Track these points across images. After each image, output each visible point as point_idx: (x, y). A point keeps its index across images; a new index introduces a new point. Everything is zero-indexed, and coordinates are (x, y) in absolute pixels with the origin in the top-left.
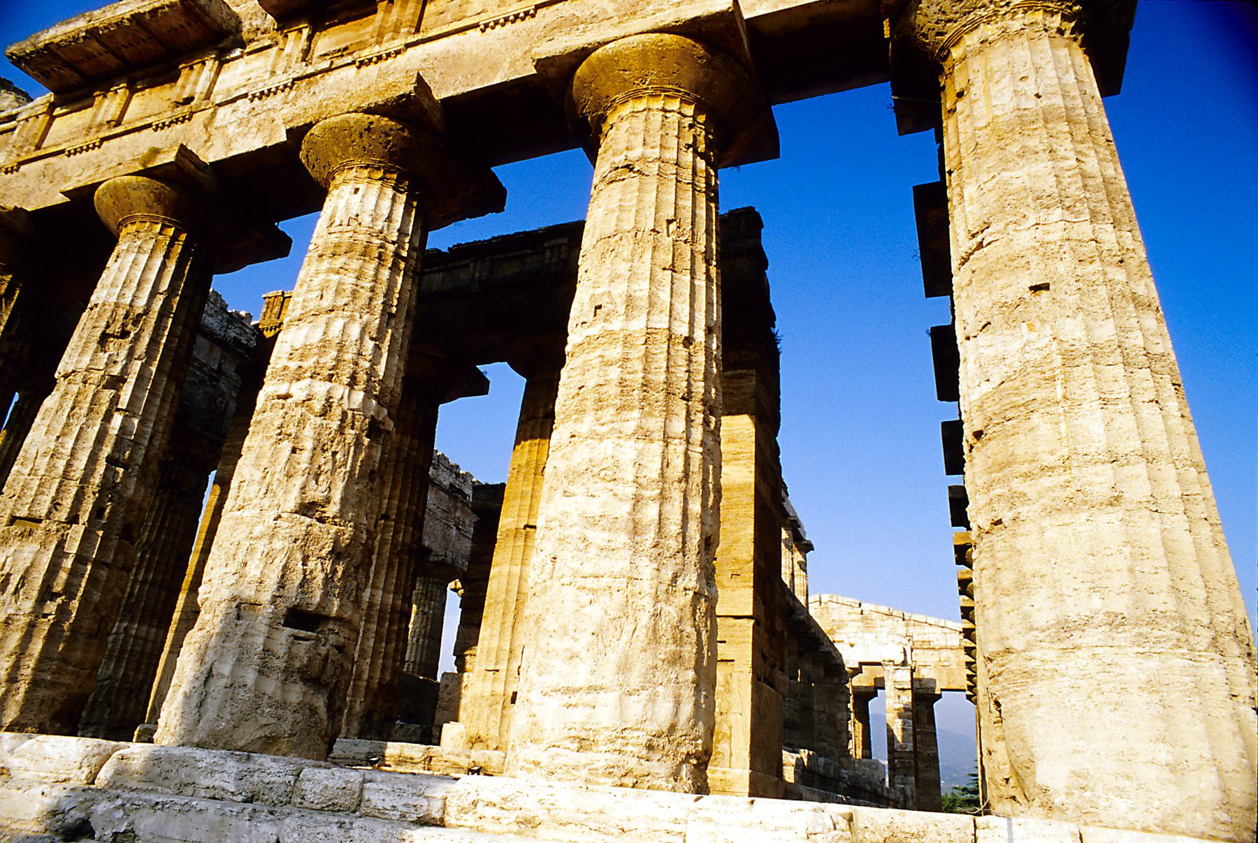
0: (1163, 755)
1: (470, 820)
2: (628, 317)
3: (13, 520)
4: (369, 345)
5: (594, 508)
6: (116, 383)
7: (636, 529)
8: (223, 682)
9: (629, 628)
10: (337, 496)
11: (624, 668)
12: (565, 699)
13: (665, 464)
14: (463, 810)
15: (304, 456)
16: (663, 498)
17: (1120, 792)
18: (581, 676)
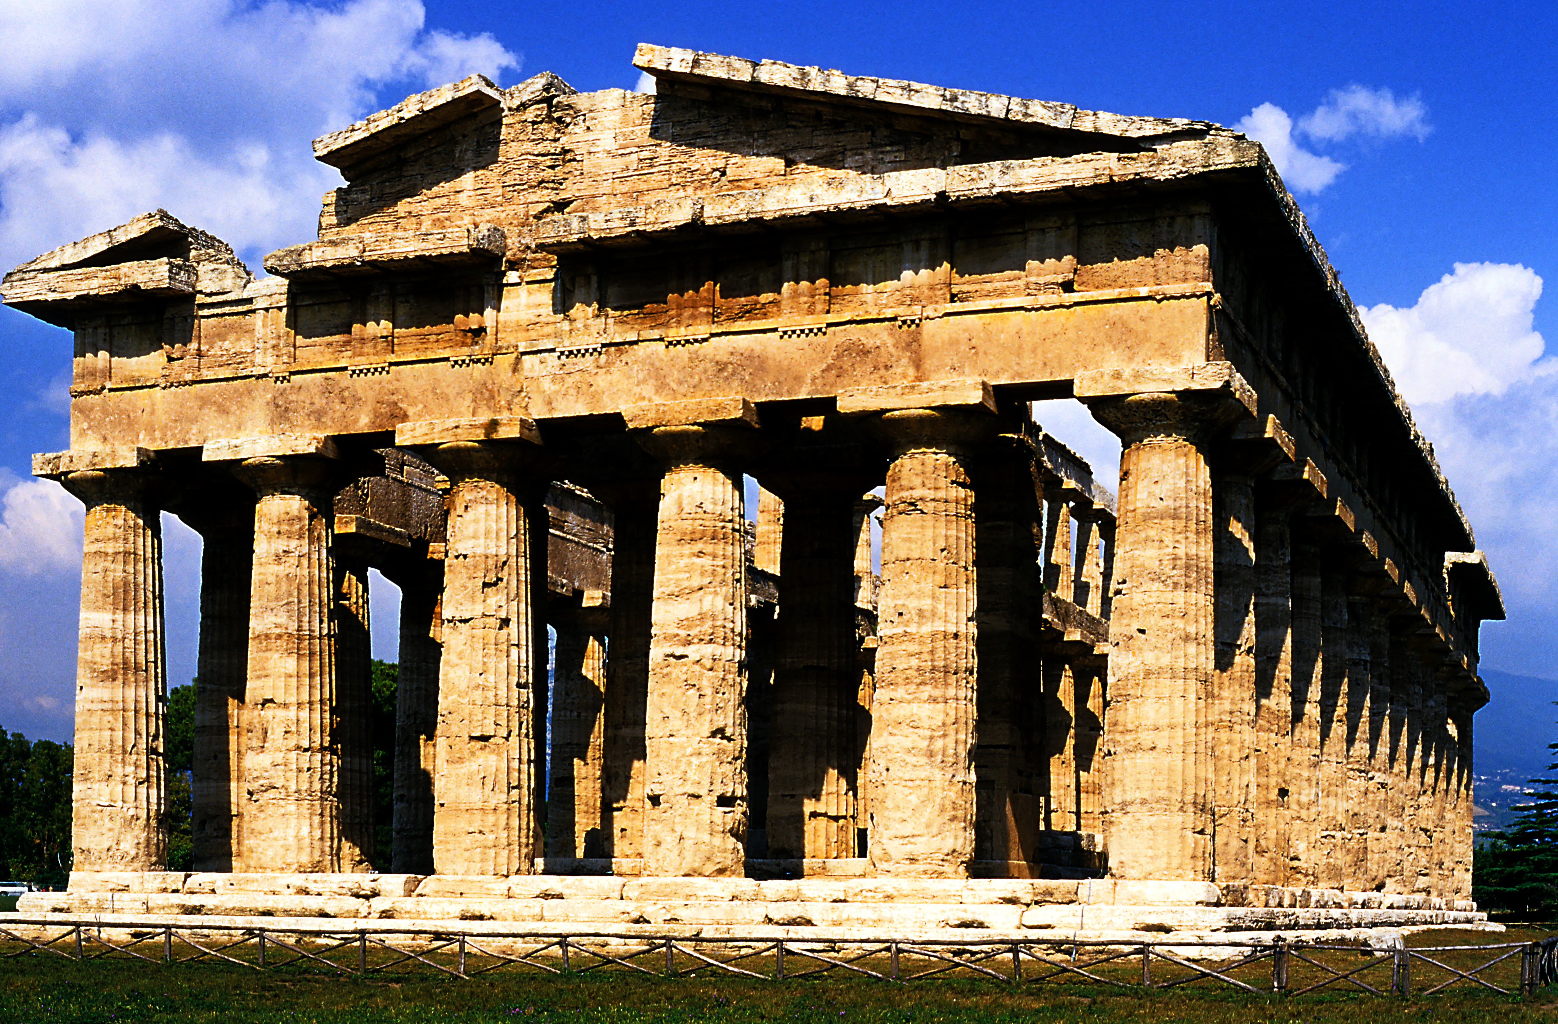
0: (1150, 853)
1: (859, 898)
2: (920, 624)
5: (908, 744)
8: (691, 842)
12: (901, 841)
14: (856, 895)
17: (1133, 868)
18: (907, 829)
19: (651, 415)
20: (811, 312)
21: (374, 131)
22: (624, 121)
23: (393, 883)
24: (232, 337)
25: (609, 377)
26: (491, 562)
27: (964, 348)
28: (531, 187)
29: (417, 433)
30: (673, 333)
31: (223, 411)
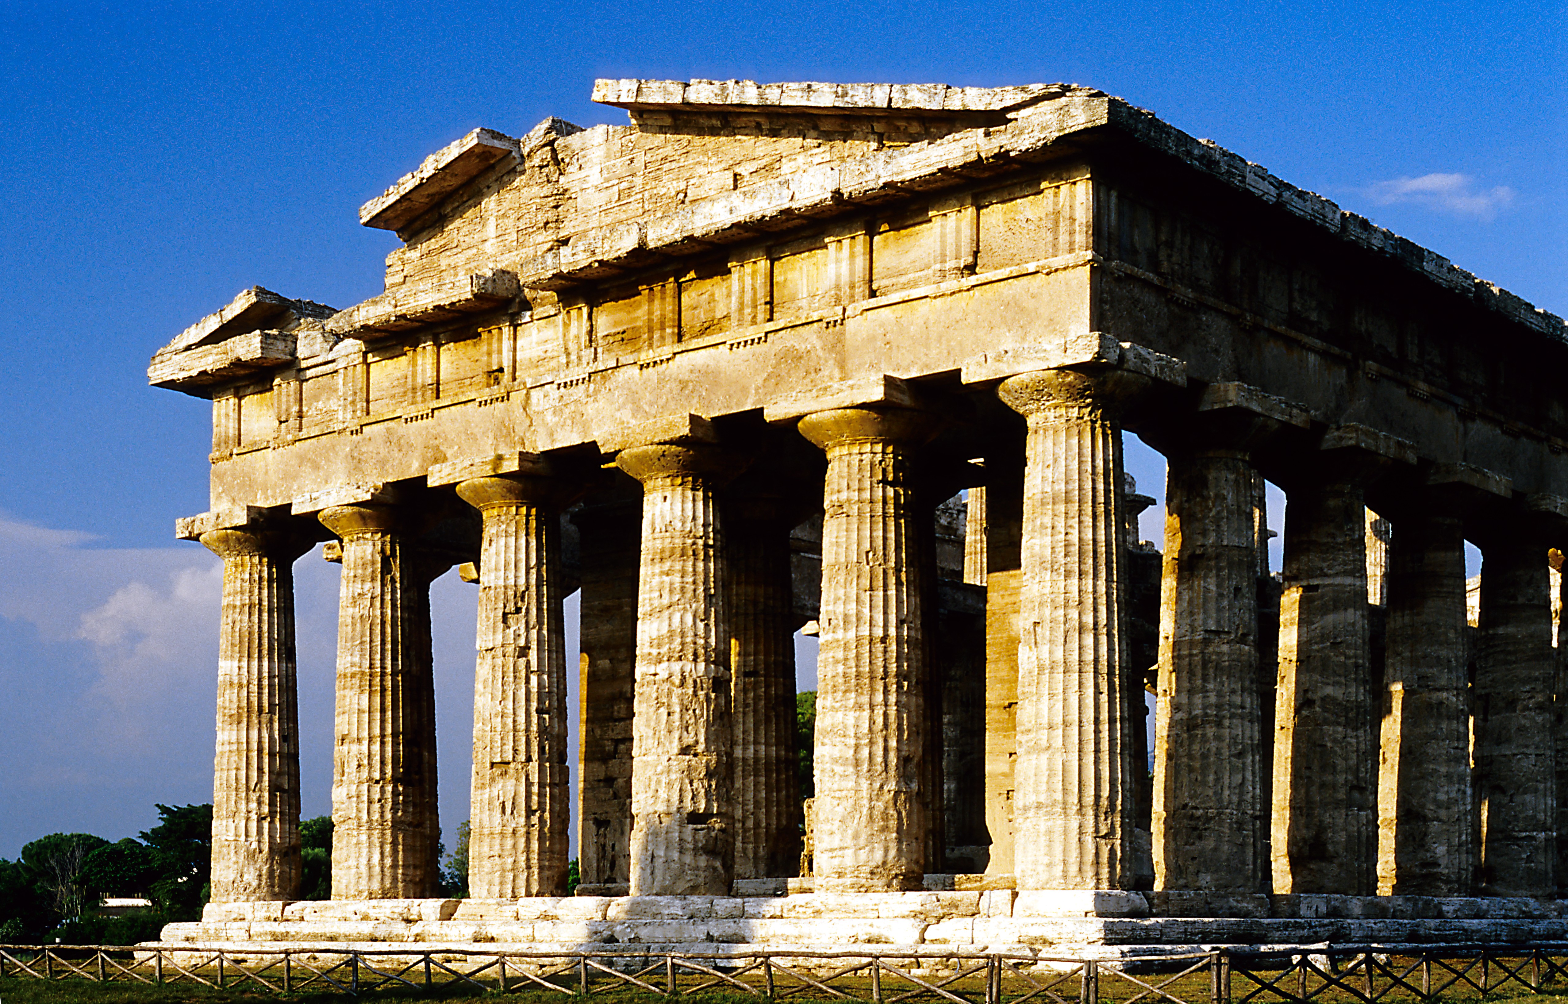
1: (793, 914)
3: (493, 765)
4: (701, 625)
5: (836, 753)
6: (523, 652)
7: (857, 763)
8: (661, 860)
9: (857, 816)
10: (702, 739)
11: (856, 836)
12: (830, 854)
13: (872, 722)
14: (789, 910)
15: (676, 716)
16: (871, 743)
18: (836, 844)
19: (618, 439)
20: (754, 322)
21: (403, 193)
22: (608, 157)
23: (431, 906)
24: (324, 397)
25: (597, 404)
26: (511, 593)
27: (880, 343)
28: (538, 229)
29: (443, 474)
30: (646, 356)
31: (316, 467)
